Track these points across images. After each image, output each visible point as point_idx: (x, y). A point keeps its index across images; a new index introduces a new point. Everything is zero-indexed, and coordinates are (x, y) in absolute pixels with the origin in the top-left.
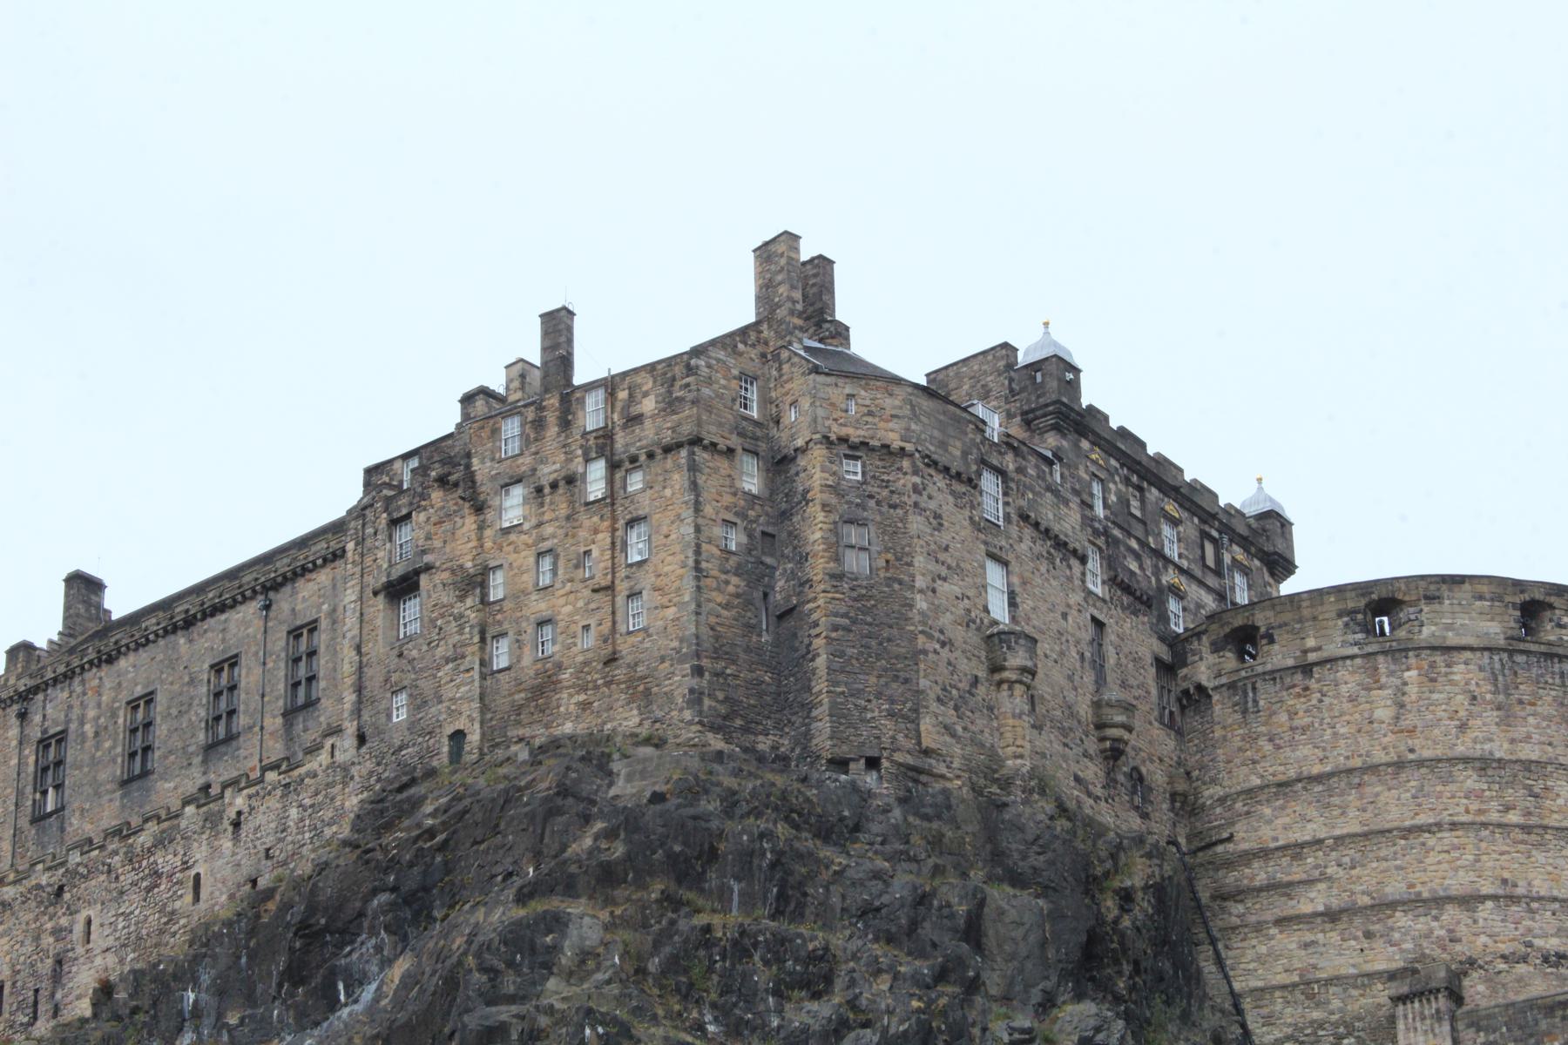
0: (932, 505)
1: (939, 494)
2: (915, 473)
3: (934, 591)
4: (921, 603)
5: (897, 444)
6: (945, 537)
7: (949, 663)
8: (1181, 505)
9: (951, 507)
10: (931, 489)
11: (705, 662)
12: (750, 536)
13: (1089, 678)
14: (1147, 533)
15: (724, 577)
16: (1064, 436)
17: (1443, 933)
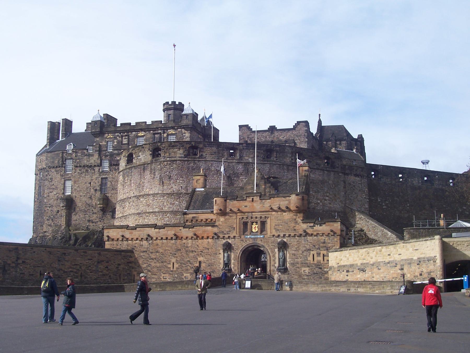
0: (50, 177)
1: (53, 173)
3: (49, 196)
4: (45, 201)
6: (53, 182)
8: (144, 131)
9: (55, 175)
10: (50, 173)
16: (97, 137)
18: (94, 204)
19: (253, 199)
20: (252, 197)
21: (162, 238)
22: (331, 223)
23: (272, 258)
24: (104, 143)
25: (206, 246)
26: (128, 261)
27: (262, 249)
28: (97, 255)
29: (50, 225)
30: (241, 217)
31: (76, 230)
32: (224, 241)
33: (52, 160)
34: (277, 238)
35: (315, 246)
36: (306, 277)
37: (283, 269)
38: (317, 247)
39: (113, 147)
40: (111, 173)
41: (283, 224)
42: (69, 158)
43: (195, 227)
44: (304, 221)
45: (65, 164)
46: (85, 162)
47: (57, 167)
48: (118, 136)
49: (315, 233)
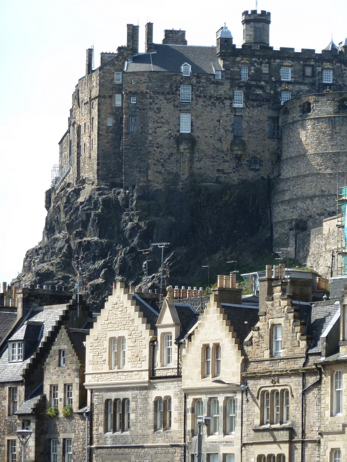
0: (157, 106)
2: (150, 98)
3: (155, 132)
4: (150, 138)
5: (145, 91)
6: (162, 114)
7: (160, 152)
8: (292, 61)
9: (165, 104)
11: (100, 161)
12: (116, 119)
13: (230, 137)
14: (271, 76)
15: (107, 134)
16: (227, 61)
17: (305, 208)
18: (225, 149)
24: (236, 69)
29: (160, 172)
31: (203, 182)
33: (159, 83)
39: (249, 76)
40: (247, 110)
42: (187, 83)
45: (180, 91)
46: (212, 92)
47: (168, 93)
48: (256, 62)
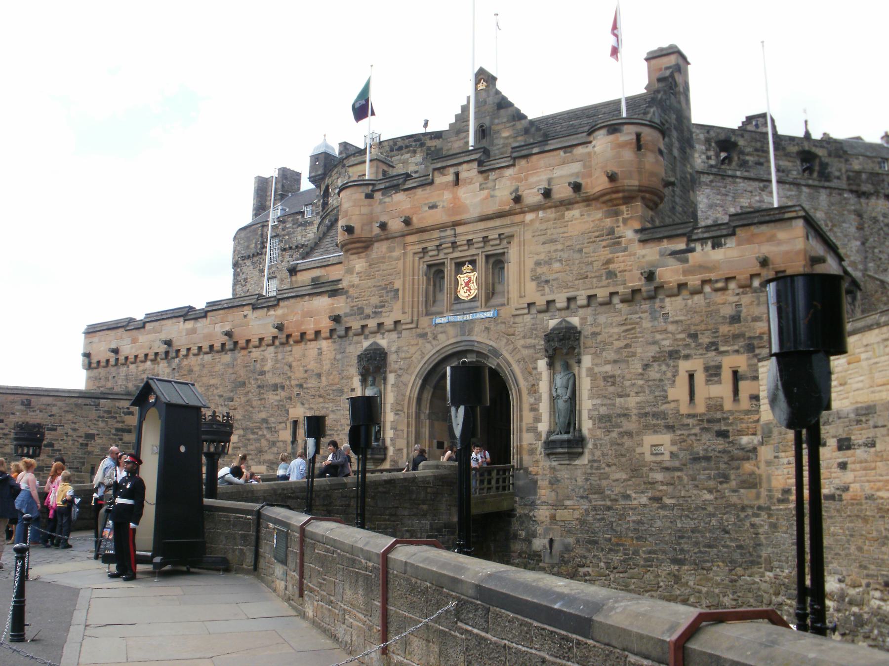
19: (457, 175)
20: (452, 170)
21: (200, 348)
22: (764, 228)
23: (527, 400)
25: (312, 365)
26: (120, 425)
27: (492, 363)
28: (19, 407)
30: (418, 248)
32: (366, 344)
34: (545, 316)
35: (694, 336)
36: (659, 476)
37: (567, 443)
38: (705, 339)
41: (565, 255)
43: (282, 304)
44: (648, 235)
49: (694, 281)
